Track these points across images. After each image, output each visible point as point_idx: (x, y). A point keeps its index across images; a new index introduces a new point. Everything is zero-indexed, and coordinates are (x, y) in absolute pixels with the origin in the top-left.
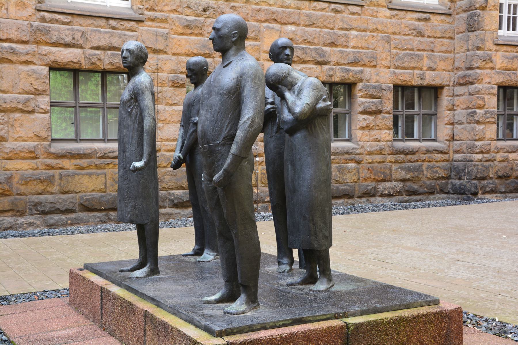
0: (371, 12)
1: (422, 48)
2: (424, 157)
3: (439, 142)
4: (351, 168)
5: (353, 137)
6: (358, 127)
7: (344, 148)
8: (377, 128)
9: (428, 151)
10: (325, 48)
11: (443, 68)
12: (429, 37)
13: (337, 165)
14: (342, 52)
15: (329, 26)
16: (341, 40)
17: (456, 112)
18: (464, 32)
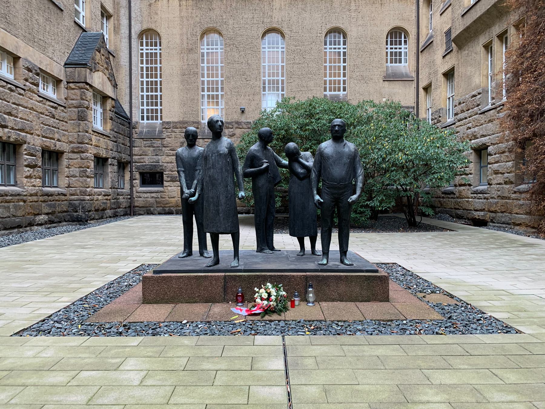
0: (29, 95)
1: (54, 126)
2: (57, 198)
3: (60, 188)
4: (21, 205)
5: (18, 183)
6: (24, 176)
7: (16, 191)
8: (34, 177)
9: (59, 194)
10: (4, 115)
11: (64, 140)
12: (57, 119)
13: (13, 204)
14: (15, 120)
15: (7, 100)
16: (14, 112)
17: (70, 169)
18: (75, 120)
